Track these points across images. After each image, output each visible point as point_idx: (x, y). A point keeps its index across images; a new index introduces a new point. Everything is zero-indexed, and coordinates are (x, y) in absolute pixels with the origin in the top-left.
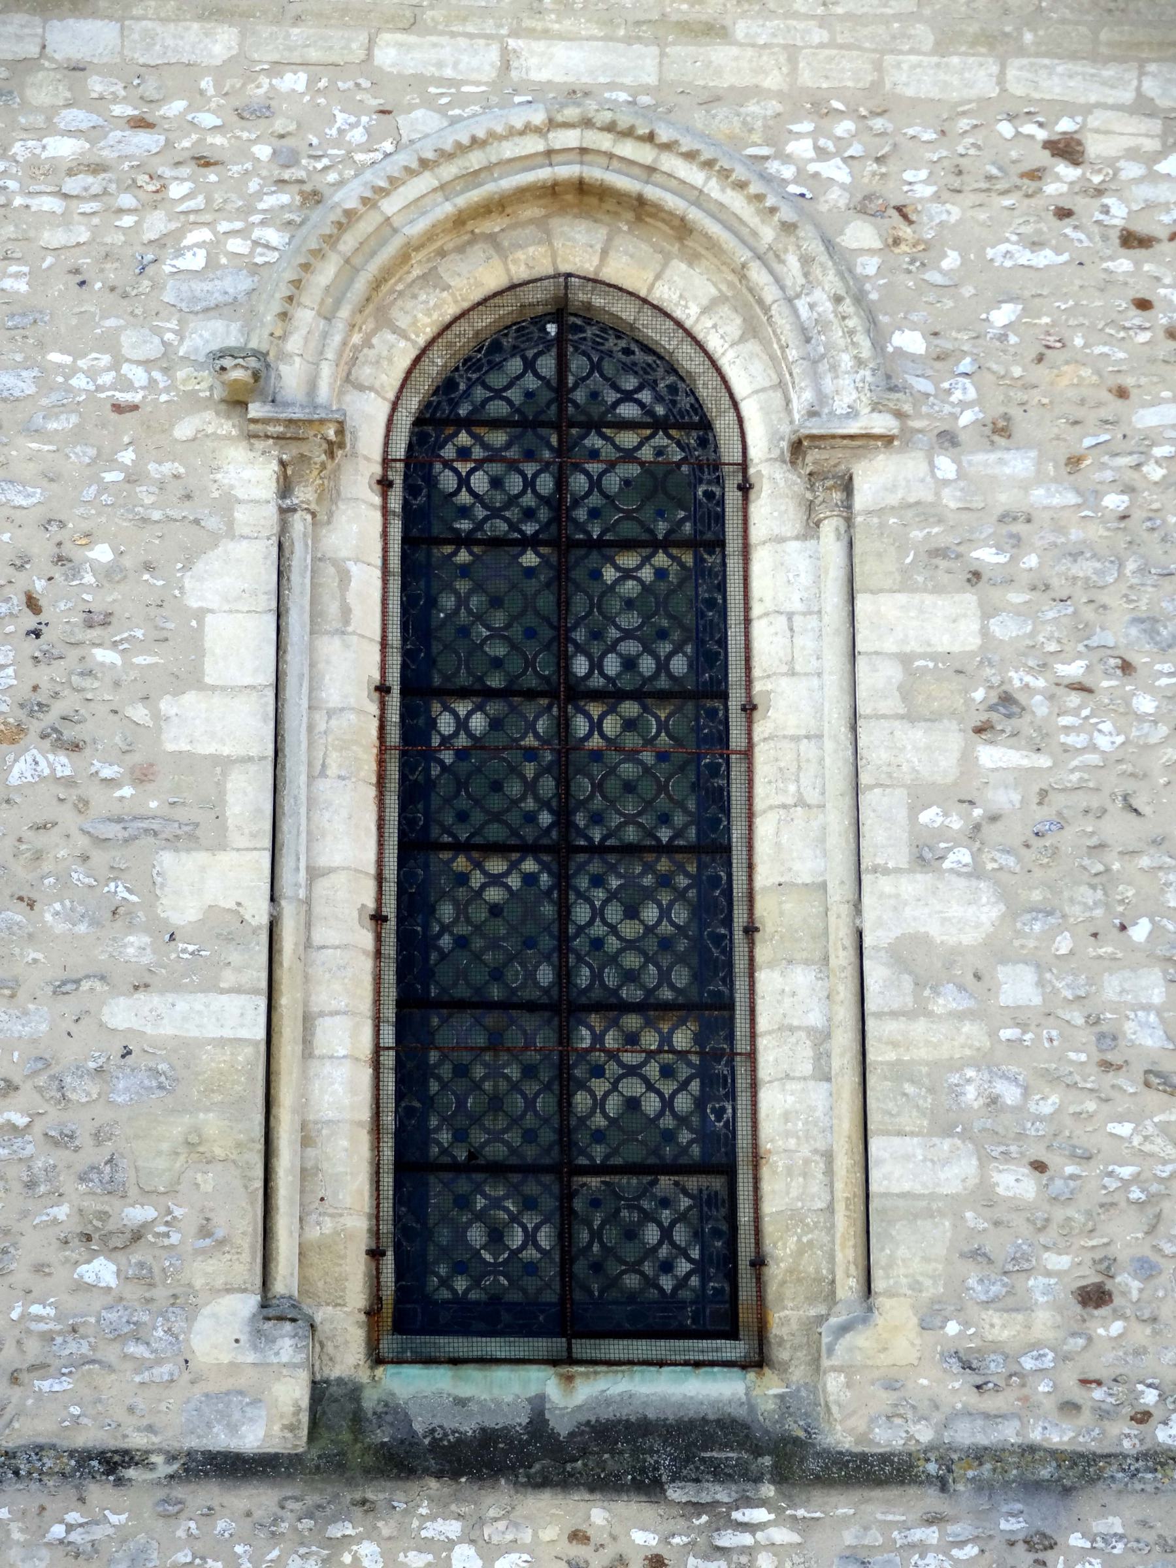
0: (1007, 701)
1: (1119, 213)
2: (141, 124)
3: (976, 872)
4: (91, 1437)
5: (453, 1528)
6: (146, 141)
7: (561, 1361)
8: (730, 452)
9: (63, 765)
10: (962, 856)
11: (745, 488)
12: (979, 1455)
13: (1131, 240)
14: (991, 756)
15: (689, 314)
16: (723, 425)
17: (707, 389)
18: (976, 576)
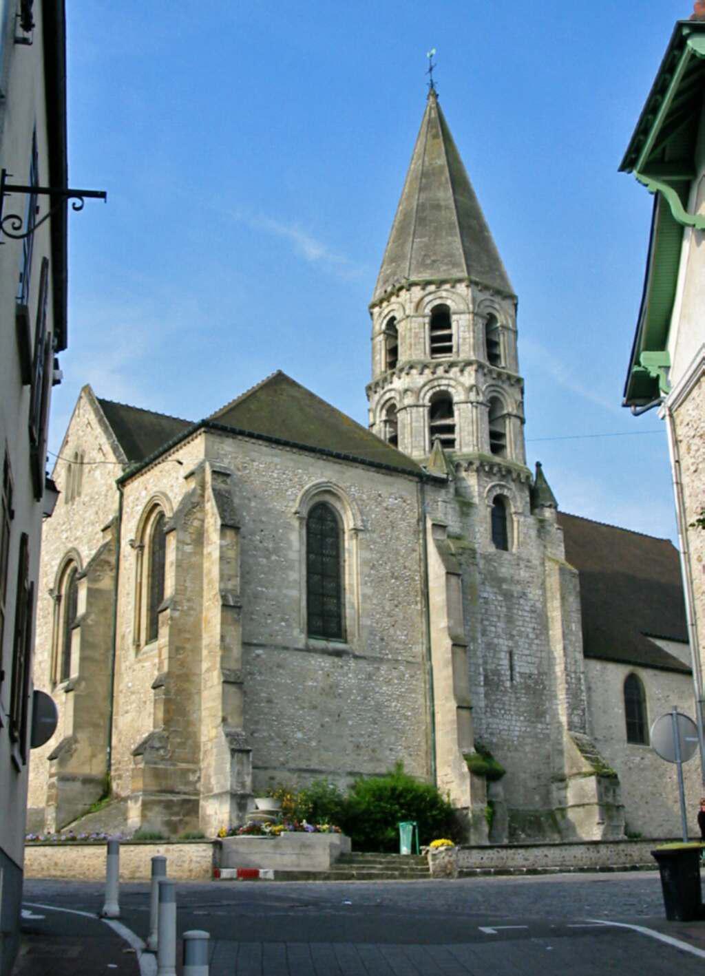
0: (374, 565)
1: (385, 505)
2: (284, 474)
3: (371, 586)
4: (284, 645)
5: (320, 660)
6: (285, 476)
7: (327, 640)
8: (341, 527)
9: (277, 558)
10: (369, 584)
11: (344, 533)
12: (372, 657)
13: (387, 509)
14: (372, 572)
15: (339, 508)
16: (340, 523)
17: (338, 518)
18: (371, 549)
